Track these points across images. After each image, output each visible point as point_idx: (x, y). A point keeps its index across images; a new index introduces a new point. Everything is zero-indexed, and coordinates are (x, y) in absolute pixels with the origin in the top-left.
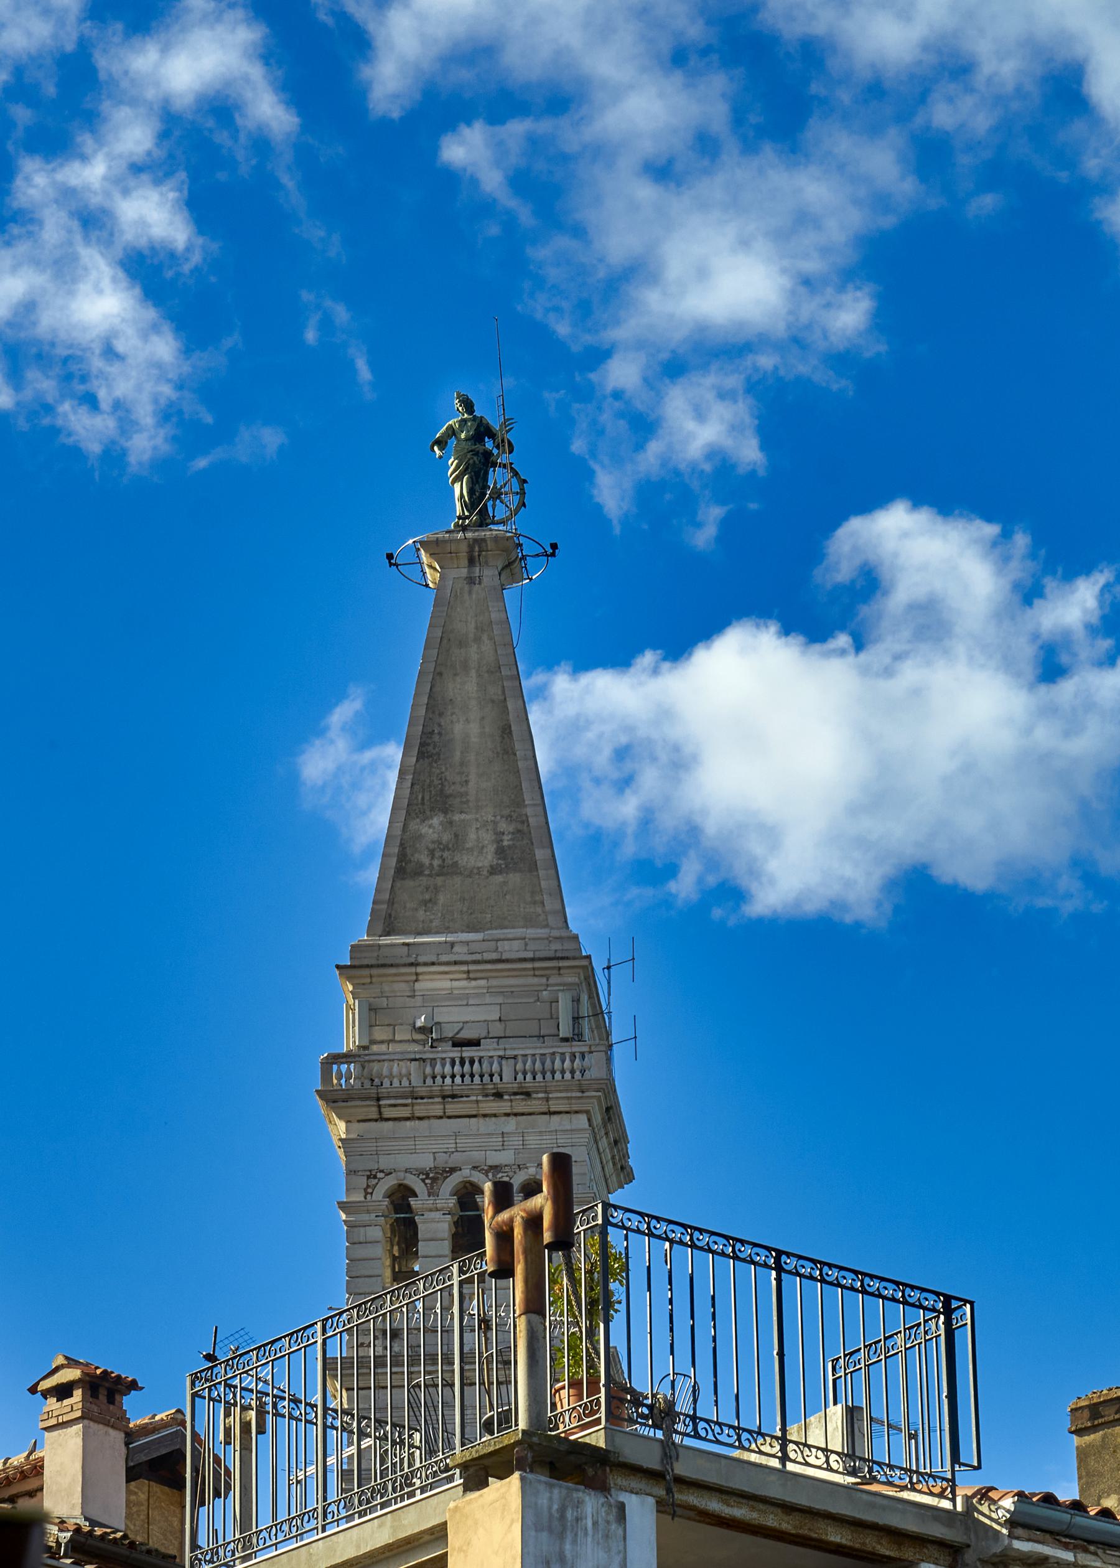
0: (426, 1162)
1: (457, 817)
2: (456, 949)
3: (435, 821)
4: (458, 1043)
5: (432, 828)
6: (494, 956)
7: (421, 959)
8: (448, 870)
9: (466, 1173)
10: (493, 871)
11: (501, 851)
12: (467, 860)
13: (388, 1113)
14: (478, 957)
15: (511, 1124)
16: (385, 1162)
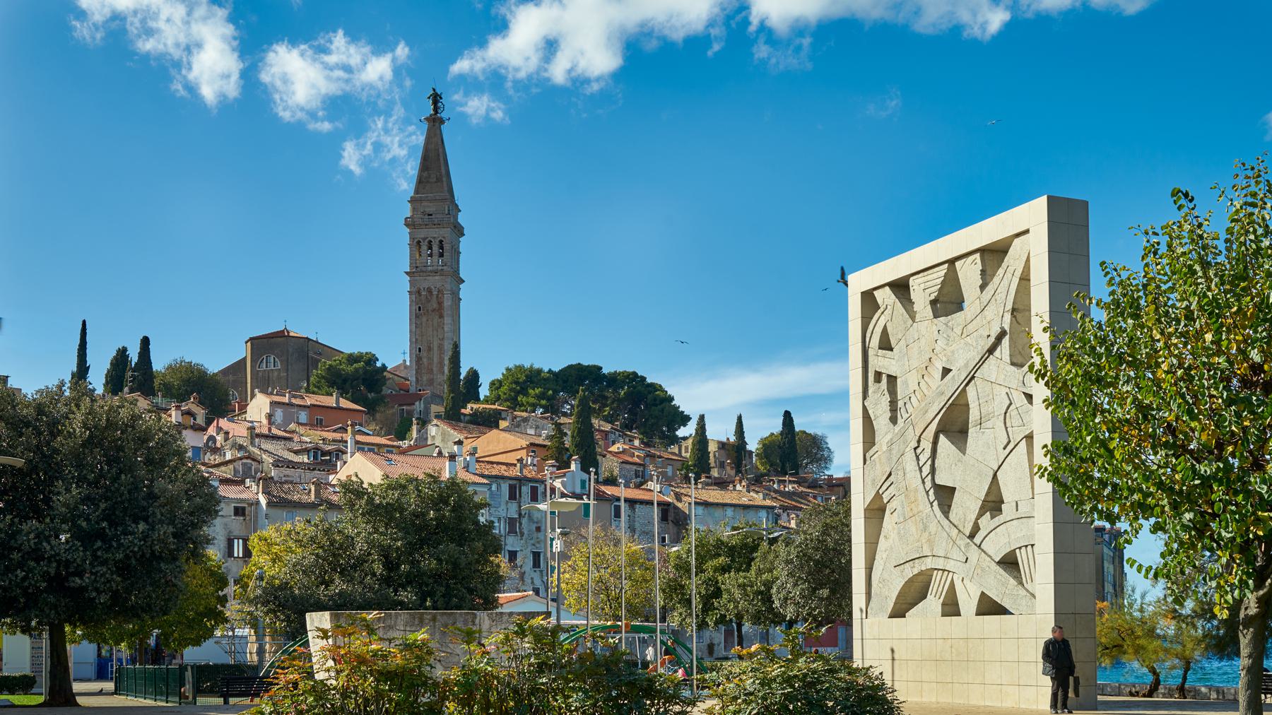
0: (423, 236)
4: (429, 215)
5: (425, 174)
8: (428, 182)
12: (431, 180)
15: (437, 230)
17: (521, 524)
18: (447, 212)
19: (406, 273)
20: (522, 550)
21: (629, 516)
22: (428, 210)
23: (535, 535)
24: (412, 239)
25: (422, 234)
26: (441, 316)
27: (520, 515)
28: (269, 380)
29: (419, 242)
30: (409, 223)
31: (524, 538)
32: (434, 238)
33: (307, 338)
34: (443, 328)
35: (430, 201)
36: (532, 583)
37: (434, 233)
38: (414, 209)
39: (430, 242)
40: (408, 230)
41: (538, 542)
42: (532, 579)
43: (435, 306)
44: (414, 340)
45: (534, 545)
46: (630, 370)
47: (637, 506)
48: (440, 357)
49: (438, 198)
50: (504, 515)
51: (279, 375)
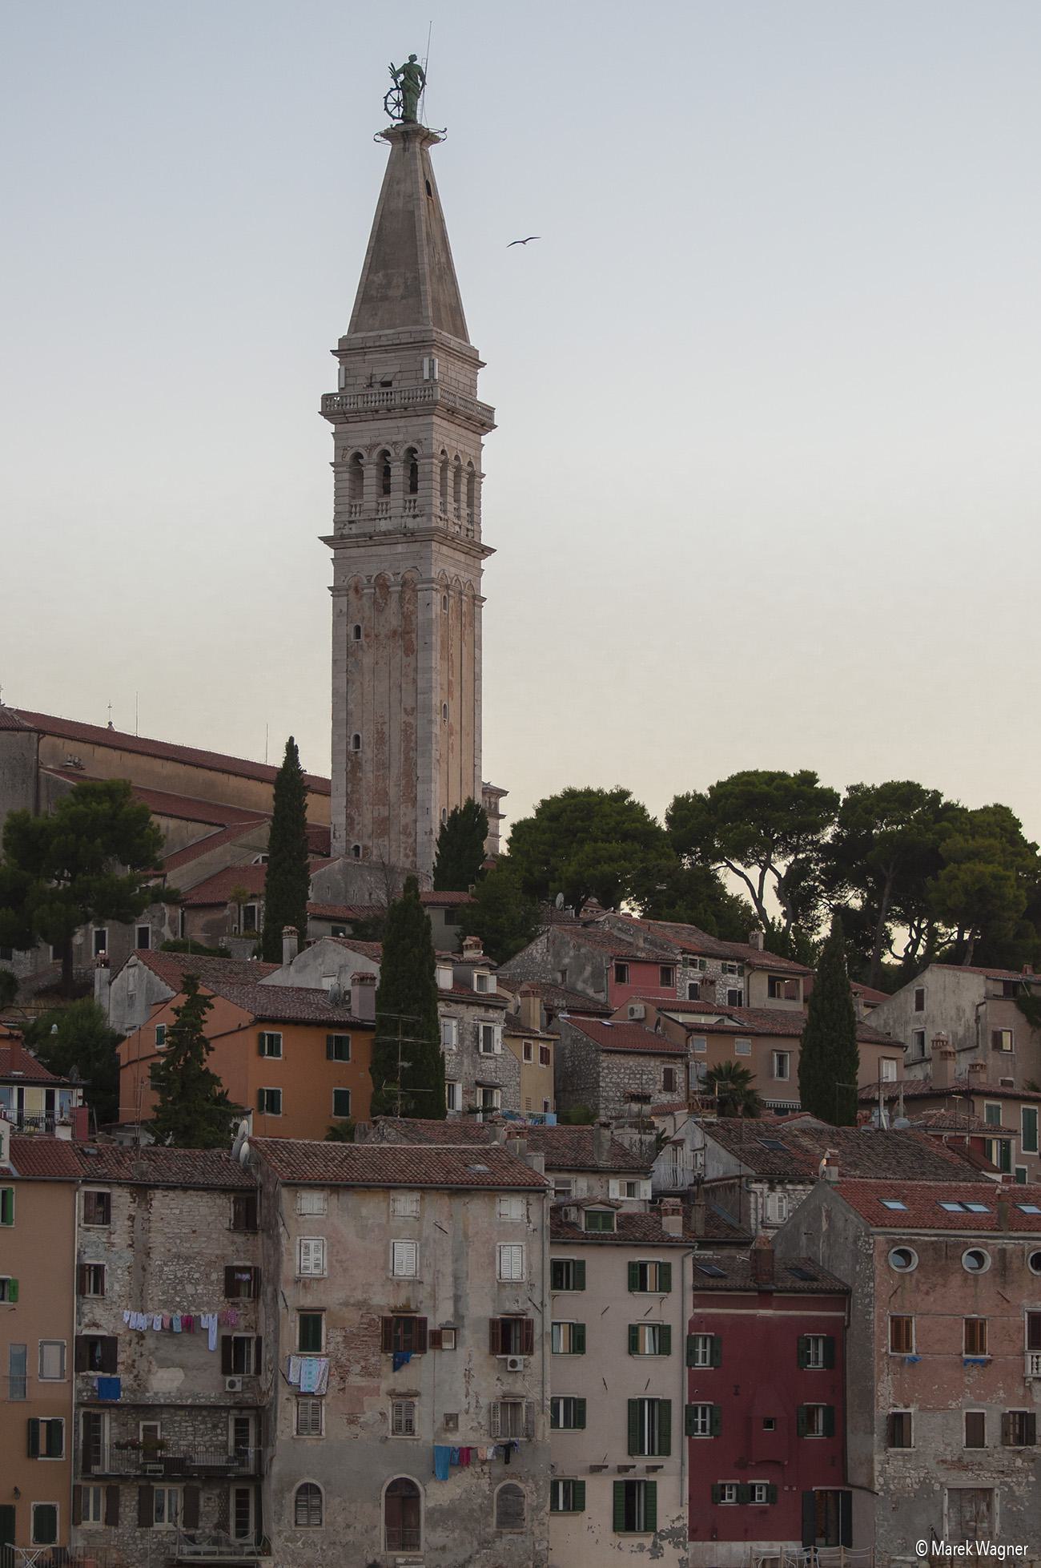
0: (367, 441)
1: (389, 271)
2: (382, 338)
3: (380, 274)
5: (379, 278)
6: (398, 342)
7: (368, 345)
8: (385, 298)
10: (403, 298)
12: (391, 293)
13: (350, 420)
14: (390, 343)
15: (401, 422)
16: (351, 442)
18: (426, 377)
19: (326, 540)
21: (131, 1218)
22: (382, 372)
25: (367, 434)
26: (409, 650)
30: (331, 408)
34: (415, 681)
35: (384, 348)
37: (393, 433)
38: (347, 374)
39: (385, 454)
40: (332, 428)
43: (395, 622)
44: (343, 715)
46: (901, 778)
47: (158, 1194)
48: (407, 759)
49: (405, 338)
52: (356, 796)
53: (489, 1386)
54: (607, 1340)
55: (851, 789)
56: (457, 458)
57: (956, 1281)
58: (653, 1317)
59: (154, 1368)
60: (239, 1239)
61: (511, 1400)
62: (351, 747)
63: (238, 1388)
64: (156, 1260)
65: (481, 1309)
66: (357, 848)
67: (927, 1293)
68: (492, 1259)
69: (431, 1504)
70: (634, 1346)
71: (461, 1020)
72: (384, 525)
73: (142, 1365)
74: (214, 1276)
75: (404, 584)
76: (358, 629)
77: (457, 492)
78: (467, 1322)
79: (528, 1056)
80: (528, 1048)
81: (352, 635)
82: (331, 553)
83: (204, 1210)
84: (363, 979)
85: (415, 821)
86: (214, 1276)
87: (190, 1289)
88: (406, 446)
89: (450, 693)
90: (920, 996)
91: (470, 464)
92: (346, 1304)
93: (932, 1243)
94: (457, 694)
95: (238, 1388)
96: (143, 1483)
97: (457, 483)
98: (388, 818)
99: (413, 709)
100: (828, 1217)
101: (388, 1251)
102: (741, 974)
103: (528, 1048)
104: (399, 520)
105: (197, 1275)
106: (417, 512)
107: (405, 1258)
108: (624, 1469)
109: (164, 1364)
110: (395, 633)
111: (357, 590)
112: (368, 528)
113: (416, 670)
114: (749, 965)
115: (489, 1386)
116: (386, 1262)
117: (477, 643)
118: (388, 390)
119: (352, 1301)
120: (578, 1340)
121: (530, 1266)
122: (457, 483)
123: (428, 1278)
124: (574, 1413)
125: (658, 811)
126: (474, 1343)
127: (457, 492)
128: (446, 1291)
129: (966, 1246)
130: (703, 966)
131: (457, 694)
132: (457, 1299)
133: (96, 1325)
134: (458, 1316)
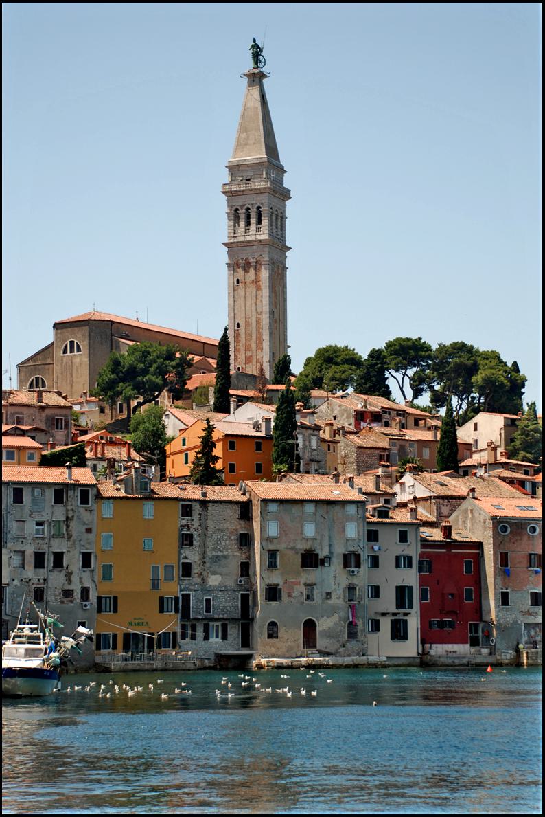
0: (240, 204)
5: (244, 135)
8: (246, 144)
9: (247, 206)
10: (254, 144)
11: (255, 140)
17: (68, 526)
20: (68, 551)
21: (200, 514)
23: (87, 536)
24: (230, 207)
26: (259, 288)
27: (67, 518)
28: (72, 366)
29: (237, 210)
31: (71, 539)
32: (252, 204)
33: (110, 321)
34: (261, 301)
36: (81, 582)
40: (226, 198)
41: (89, 543)
42: (81, 578)
45: (83, 546)
47: (211, 504)
50: (49, 518)
51: (81, 360)
52: (238, 348)
53: (344, 580)
54: (387, 561)
55: (440, 345)
56: (277, 211)
57: (525, 538)
58: (406, 553)
59: (210, 575)
60: (242, 522)
61: (352, 587)
62: (236, 328)
63: (243, 583)
64: (210, 531)
65: (340, 550)
66: (239, 368)
67: (514, 543)
68: (344, 530)
69: (321, 629)
70: (398, 565)
71: (304, 435)
72: (249, 238)
73: (205, 574)
74: (233, 538)
75: (257, 262)
76: (238, 280)
77: (277, 225)
78: (334, 555)
79: (329, 450)
80: (329, 446)
81: (236, 282)
82: (226, 249)
83: (229, 511)
84: (268, 421)
85: (262, 357)
86: (233, 538)
87: (223, 543)
88: (257, 206)
89: (275, 306)
90: (476, 425)
91: (281, 213)
92: (287, 548)
93: (516, 522)
94: (278, 306)
95: (243, 583)
96: (206, 622)
97: (277, 221)
98: (251, 356)
99: (261, 313)
100: (472, 512)
101: (303, 526)
102: (404, 417)
103: (329, 446)
104: (254, 236)
105: (226, 537)
106: (261, 232)
107: (310, 530)
108: (394, 614)
109: (214, 573)
110: (253, 281)
111: (237, 264)
112: (242, 239)
113: (262, 297)
114: (407, 413)
115: (344, 580)
116: (302, 531)
117: (285, 286)
118: (248, 182)
119: (289, 547)
120: (375, 562)
121: (359, 532)
122: (277, 221)
123: (319, 537)
124: (375, 592)
125: (364, 354)
126: (337, 563)
127: (277, 225)
128: (326, 542)
129: (530, 524)
130: (389, 413)
131: (278, 306)
132: (330, 545)
133: (186, 558)
134: (331, 553)
